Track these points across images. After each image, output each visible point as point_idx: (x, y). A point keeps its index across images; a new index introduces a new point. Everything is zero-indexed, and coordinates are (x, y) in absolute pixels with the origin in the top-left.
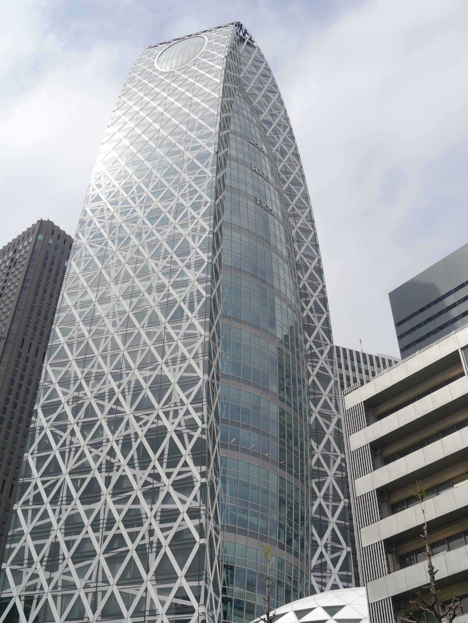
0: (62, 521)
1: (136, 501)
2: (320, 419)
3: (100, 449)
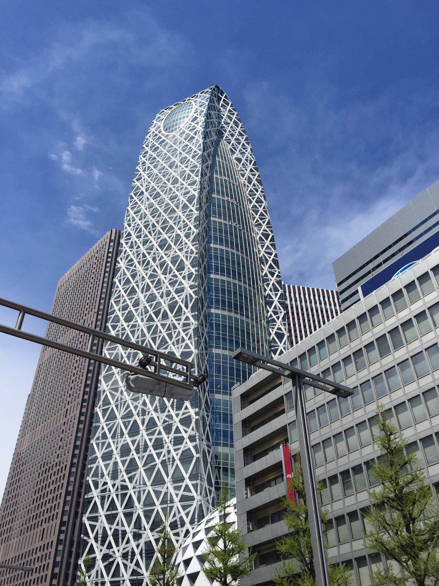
0: (119, 449)
1: (160, 433)
3: (138, 402)
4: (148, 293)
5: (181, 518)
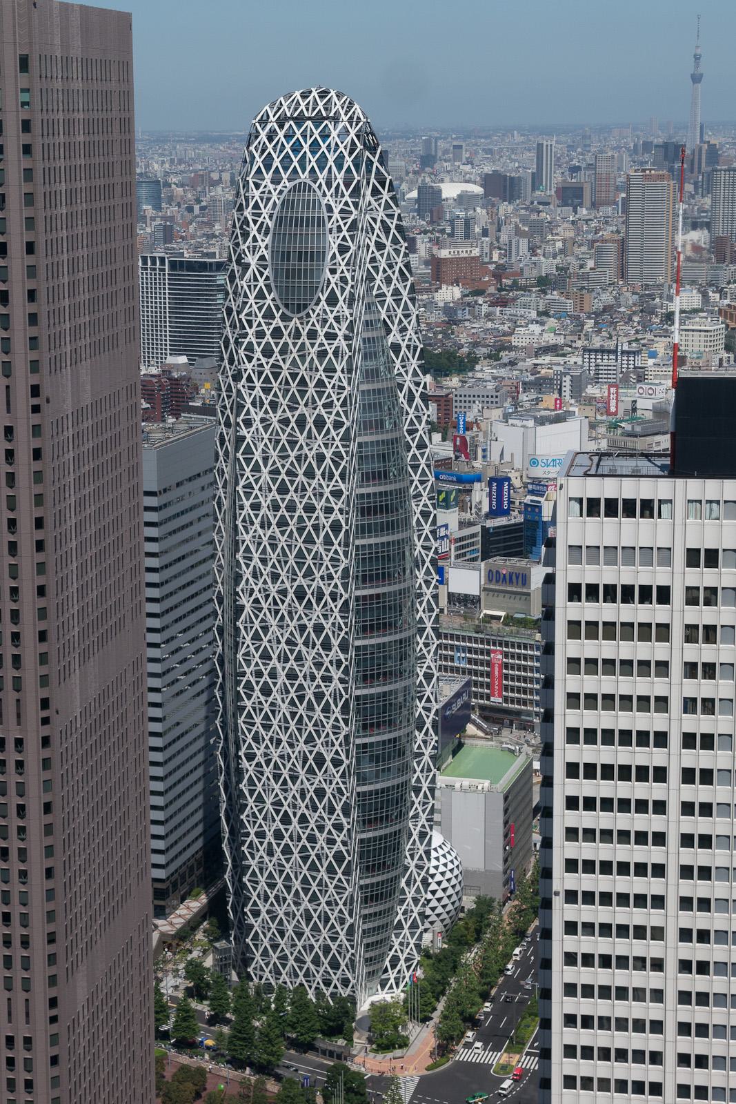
2: (423, 713)
4: (288, 666)
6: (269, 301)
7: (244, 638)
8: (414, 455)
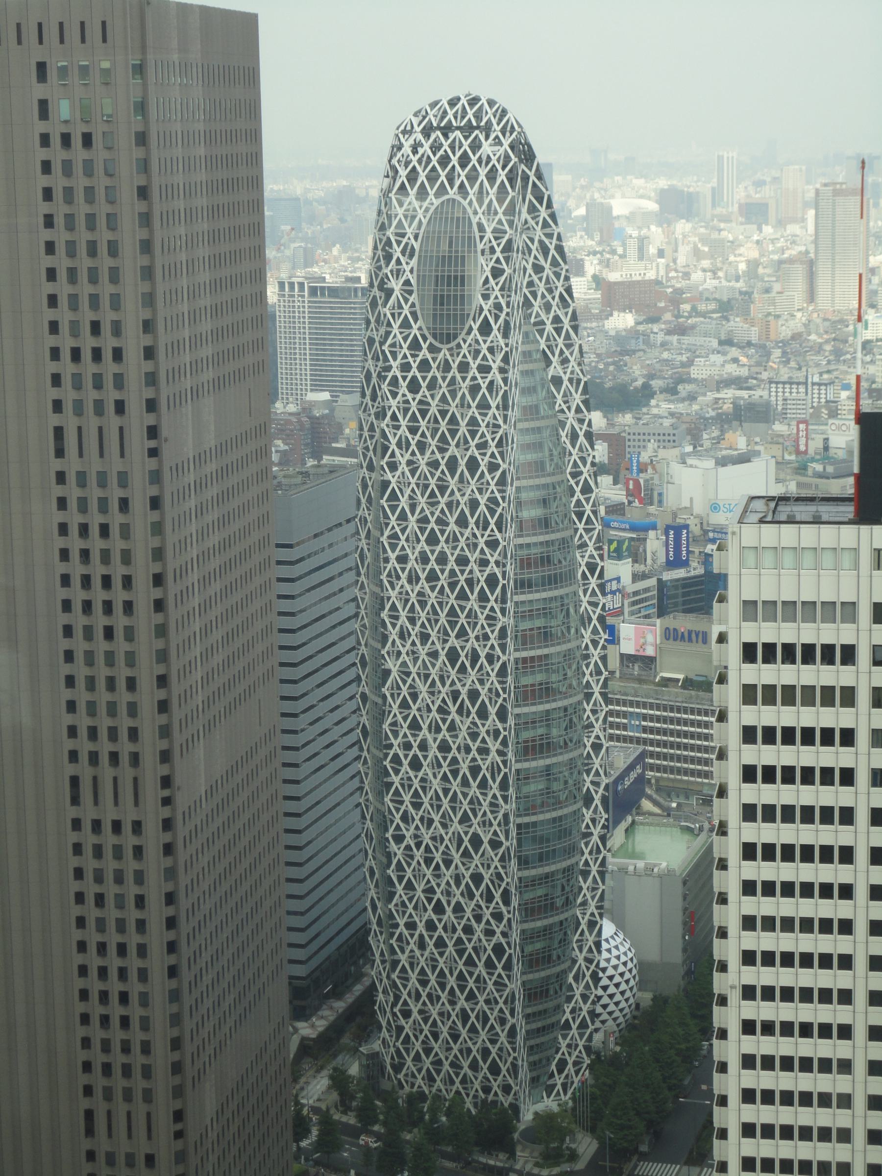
2: (592, 788)
4: (440, 737)
5: (495, 998)
6: (415, 331)
7: (390, 706)
8: (579, 501)
